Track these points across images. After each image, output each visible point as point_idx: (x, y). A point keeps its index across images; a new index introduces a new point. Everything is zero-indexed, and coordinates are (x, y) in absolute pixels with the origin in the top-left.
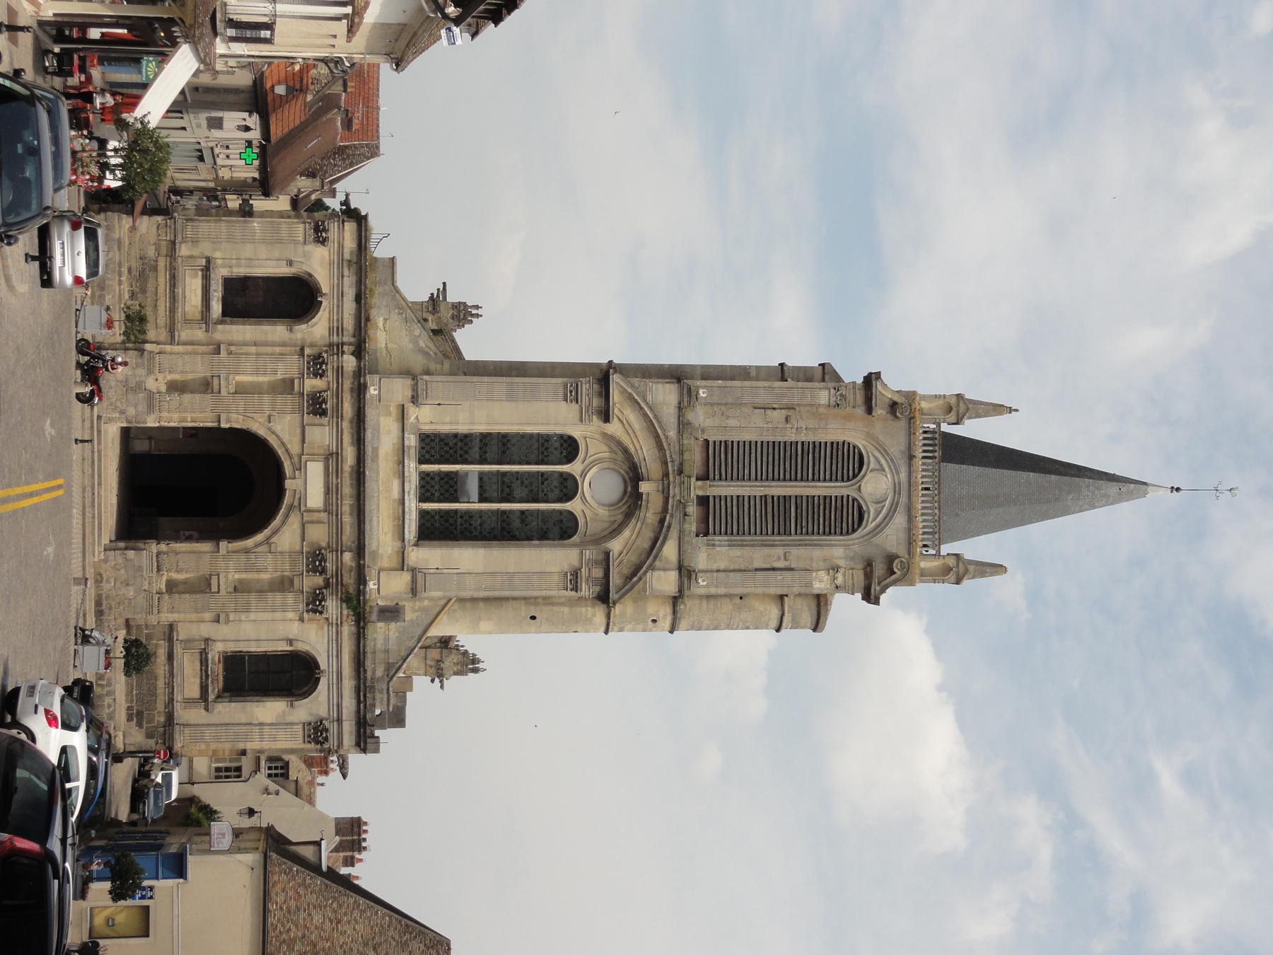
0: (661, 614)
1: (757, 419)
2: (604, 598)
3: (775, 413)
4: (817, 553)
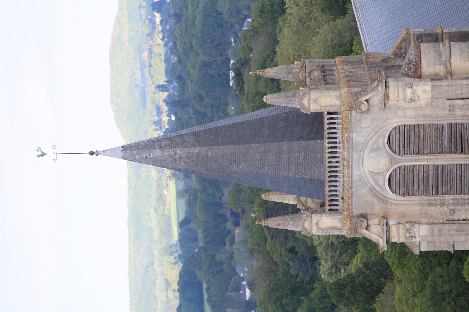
4: (428, 112)
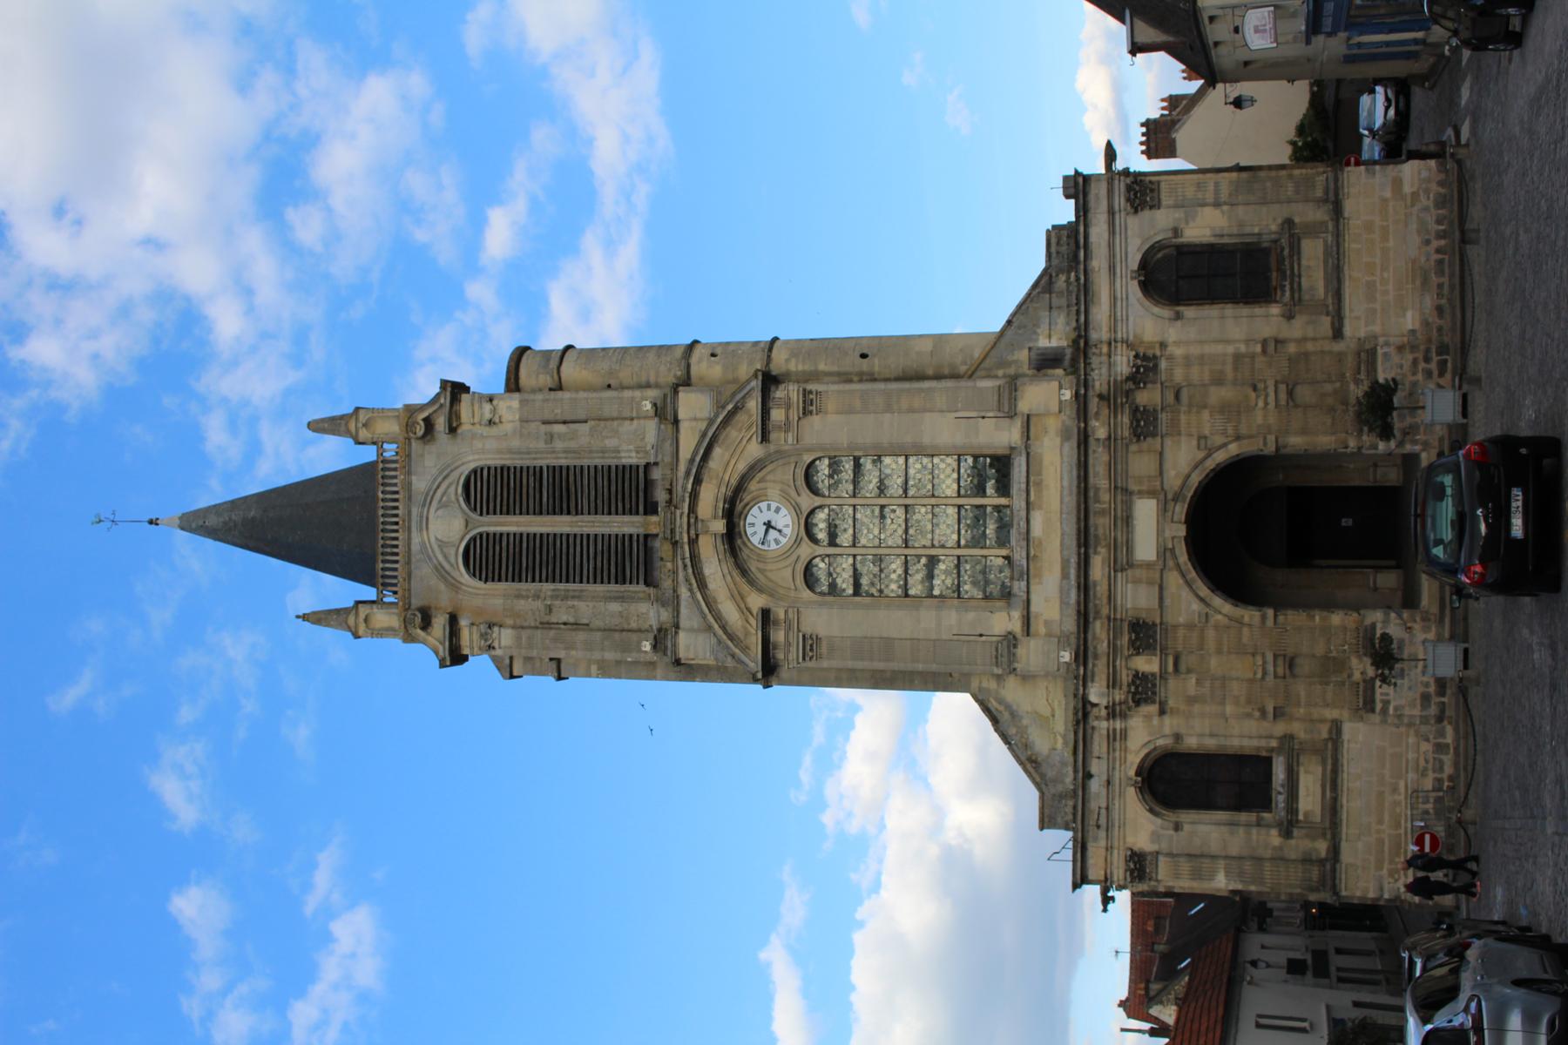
0: (704, 365)
1: (584, 610)
2: (770, 380)
3: (564, 618)
4: (515, 443)
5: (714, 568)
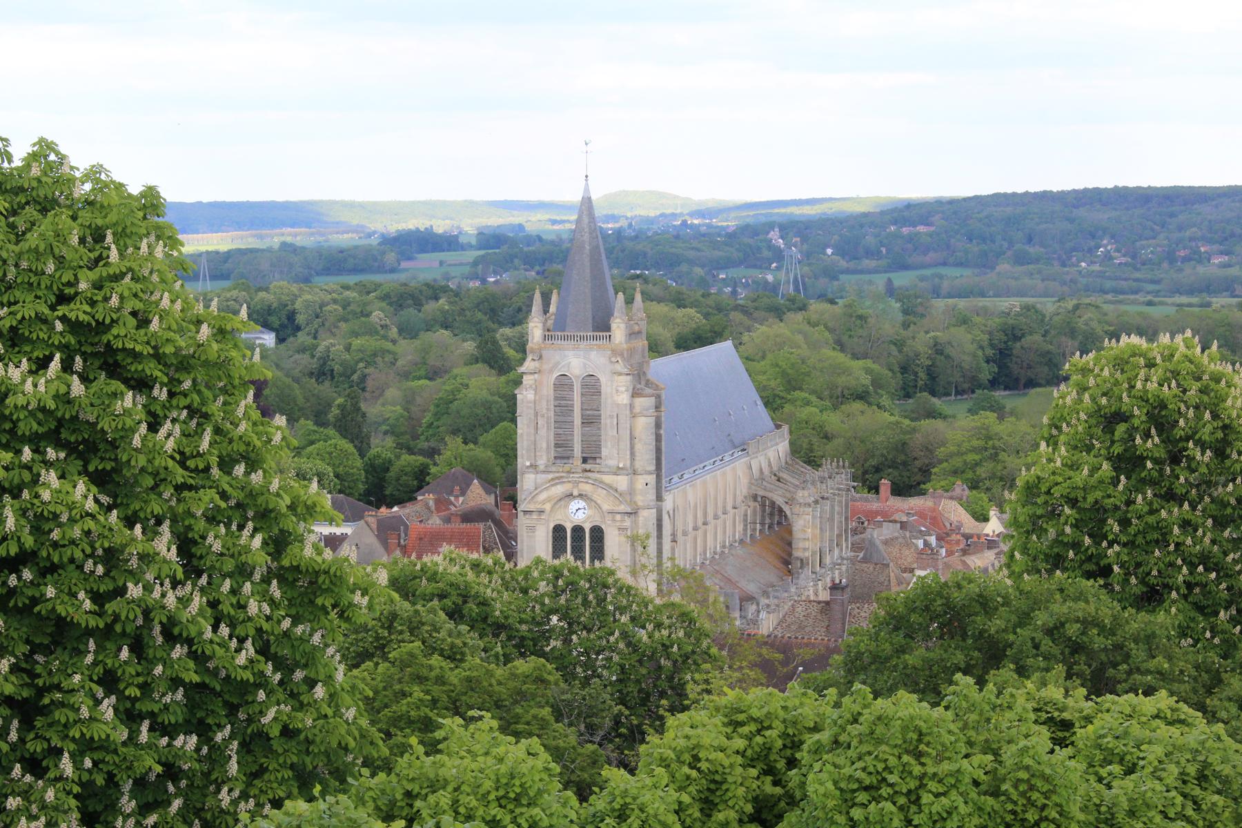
1: (543, 432)
4: (609, 401)
5: (559, 490)
